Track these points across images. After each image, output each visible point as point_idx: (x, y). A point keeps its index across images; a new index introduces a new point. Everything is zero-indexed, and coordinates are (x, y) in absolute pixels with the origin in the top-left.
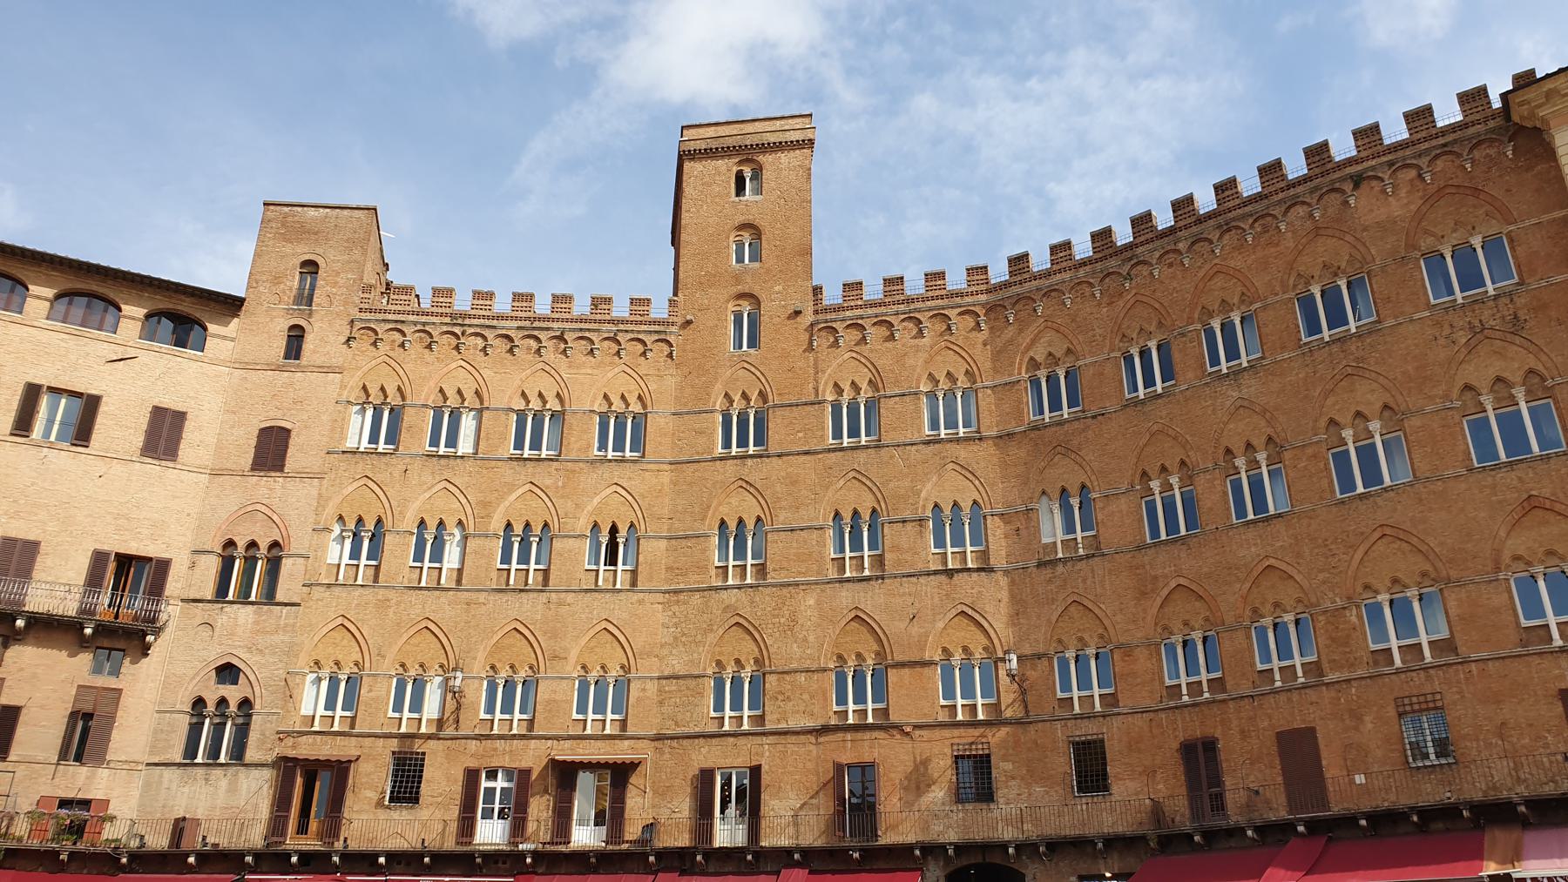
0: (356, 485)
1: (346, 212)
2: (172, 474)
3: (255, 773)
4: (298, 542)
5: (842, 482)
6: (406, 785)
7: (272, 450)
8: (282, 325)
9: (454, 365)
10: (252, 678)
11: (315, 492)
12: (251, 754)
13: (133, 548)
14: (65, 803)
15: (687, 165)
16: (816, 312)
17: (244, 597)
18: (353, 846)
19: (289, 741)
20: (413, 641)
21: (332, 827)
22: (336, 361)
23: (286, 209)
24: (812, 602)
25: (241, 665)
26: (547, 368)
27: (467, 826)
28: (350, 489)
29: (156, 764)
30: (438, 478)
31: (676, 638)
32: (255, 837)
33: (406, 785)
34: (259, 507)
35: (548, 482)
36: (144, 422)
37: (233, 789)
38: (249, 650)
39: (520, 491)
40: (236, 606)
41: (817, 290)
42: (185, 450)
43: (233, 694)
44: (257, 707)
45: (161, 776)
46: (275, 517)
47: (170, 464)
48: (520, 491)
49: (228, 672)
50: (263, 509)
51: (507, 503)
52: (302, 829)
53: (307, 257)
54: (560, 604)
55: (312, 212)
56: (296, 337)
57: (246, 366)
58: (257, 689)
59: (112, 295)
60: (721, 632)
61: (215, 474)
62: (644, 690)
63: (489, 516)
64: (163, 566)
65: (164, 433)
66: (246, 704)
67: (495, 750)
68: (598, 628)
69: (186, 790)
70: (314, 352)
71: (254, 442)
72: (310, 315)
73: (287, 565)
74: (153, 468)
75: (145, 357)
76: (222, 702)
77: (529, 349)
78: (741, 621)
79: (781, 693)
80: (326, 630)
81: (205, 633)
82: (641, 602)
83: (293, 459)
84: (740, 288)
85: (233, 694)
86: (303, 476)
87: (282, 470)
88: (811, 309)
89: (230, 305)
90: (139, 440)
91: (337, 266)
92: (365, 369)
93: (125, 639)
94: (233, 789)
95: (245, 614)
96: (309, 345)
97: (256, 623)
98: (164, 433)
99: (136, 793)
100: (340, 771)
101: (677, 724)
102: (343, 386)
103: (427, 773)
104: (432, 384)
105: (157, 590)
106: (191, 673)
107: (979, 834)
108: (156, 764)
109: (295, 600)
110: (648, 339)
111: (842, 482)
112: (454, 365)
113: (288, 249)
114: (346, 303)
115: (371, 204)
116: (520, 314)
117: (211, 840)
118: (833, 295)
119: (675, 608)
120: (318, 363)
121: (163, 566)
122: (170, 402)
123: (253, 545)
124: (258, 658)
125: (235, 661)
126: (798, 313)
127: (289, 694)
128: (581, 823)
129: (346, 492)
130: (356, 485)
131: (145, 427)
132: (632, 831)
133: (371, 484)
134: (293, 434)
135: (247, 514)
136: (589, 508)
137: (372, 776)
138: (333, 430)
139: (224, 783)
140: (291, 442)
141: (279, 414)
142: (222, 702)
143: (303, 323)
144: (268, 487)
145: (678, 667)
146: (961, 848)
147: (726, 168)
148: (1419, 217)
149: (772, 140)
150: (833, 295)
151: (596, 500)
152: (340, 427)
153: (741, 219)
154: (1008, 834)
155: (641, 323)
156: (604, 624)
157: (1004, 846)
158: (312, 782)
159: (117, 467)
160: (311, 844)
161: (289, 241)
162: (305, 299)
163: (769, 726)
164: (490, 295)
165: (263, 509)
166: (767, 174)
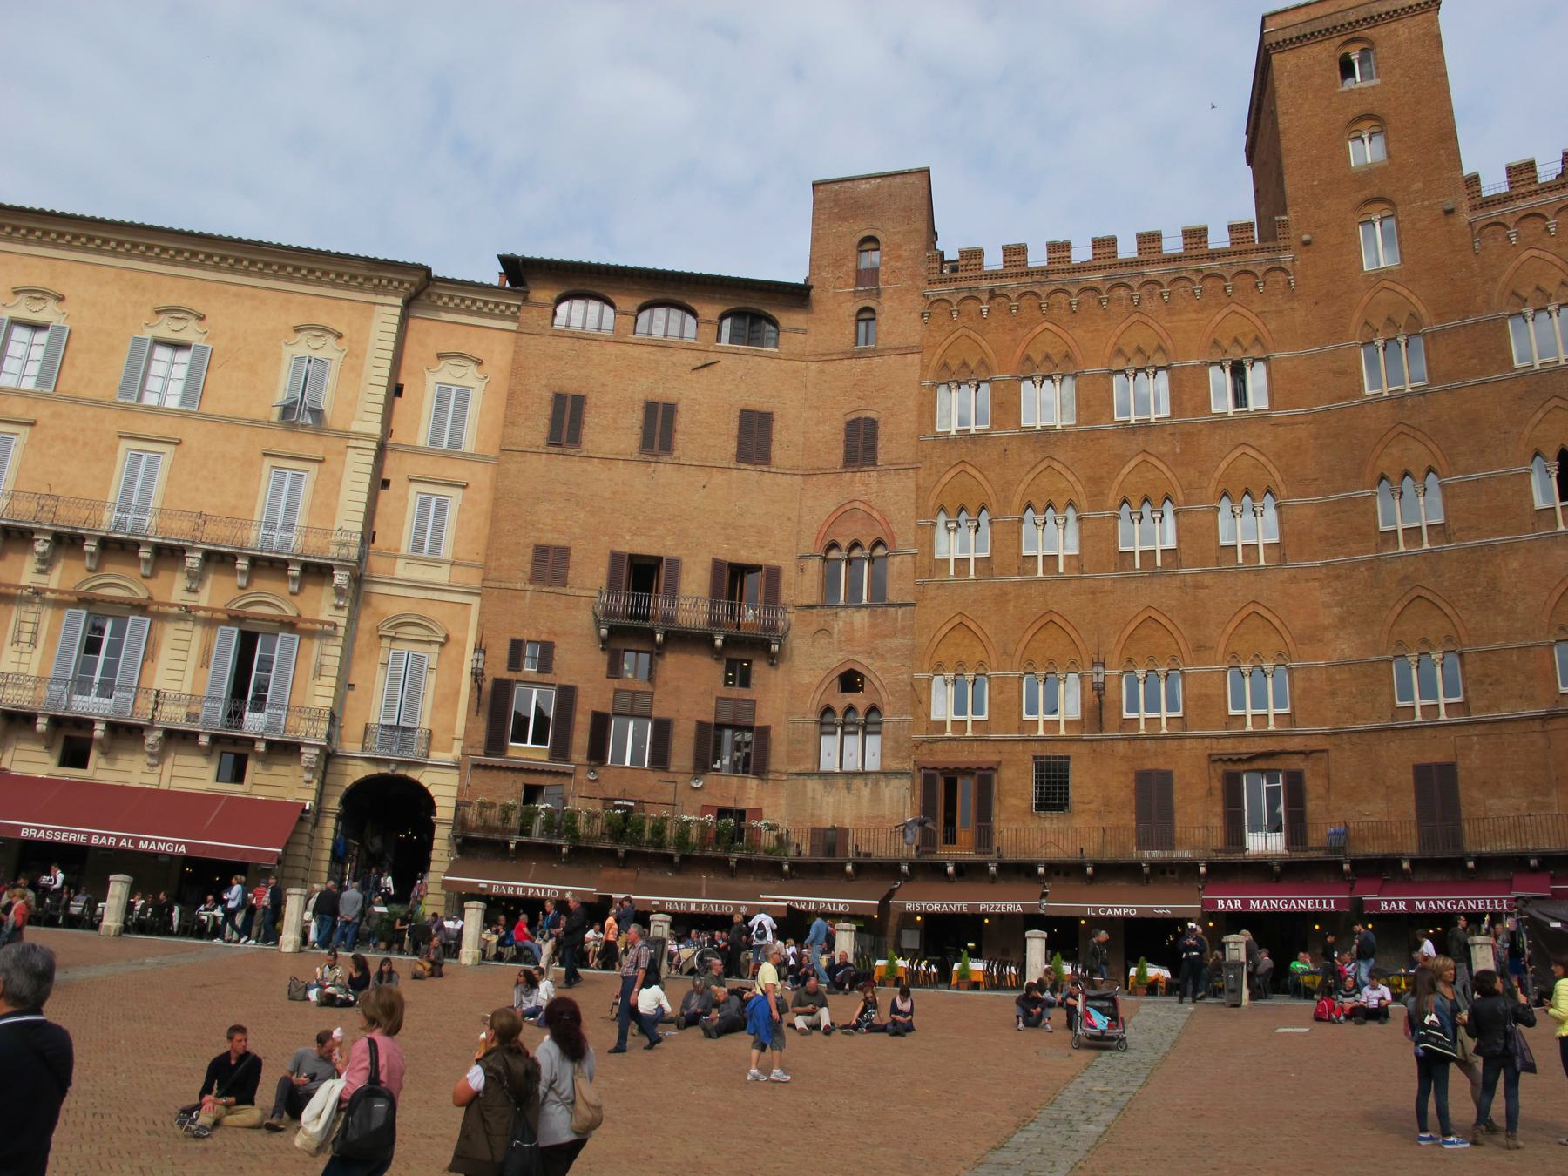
0: (953, 472)
1: (898, 180)
2: (767, 478)
3: (895, 782)
4: (905, 539)
5: (1540, 414)
6: (1053, 790)
7: (861, 442)
8: (852, 308)
9: (1038, 329)
10: (877, 684)
11: (911, 484)
13: (744, 556)
14: (722, 813)
15: (1276, 58)
16: (1474, 208)
17: (854, 602)
18: (1009, 857)
19: (925, 748)
20: (1040, 636)
21: (984, 837)
22: (915, 340)
23: (837, 187)
24: (1515, 565)
25: (864, 672)
26: (1144, 319)
28: (948, 477)
29: (799, 774)
30: (1040, 456)
31: (1342, 619)
32: (903, 849)
33: (1053, 790)
34: (857, 504)
35: (1163, 449)
36: (734, 427)
37: (876, 798)
38: (869, 654)
39: (1133, 463)
40: (850, 611)
41: (1474, 180)
42: (776, 452)
43: (859, 700)
44: (887, 713)
45: (805, 786)
46: (875, 514)
47: (765, 468)
48: (1133, 463)
49: (850, 681)
50: (861, 506)
51: (1120, 478)
52: (950, 839)
53: (866, 234)
54: (1198, 586)
55: (864, 186)
57: (823, 357)
58: (884, 695)
60: (1398, 609)
61: (809, 474)
62: (1310, 679)
63: (1102, 493)
64: (774, 574)
65: (754, 436)
66: (873, 709)
67: (1146, 751)
68: (1245, 612)
69: (831, 799)
70: (889, 334)
71: (841, 437)
72: (878, 293)
73: (894, 564)
74: (751, 474)
75: (726, 361)
76: (850, 709)
77: (1120, 299)
78: (1423, 593)
79: (1487, 675)
80: (945, 630)
81: (823, 641)
82: (1293, 579)
83: (886, 450)
84: (1366, 193)
86: (897, 468)
87: (875, 464)
88: (1465, 205)
89: (797, 296)
90: (732, 447)
91: (898, 239)
92: (945, 345)
94: (876, 798)
95: (860, 618)
96: (884, 322)
97: (873, 626)
98: (754, 436)
99: (783, 802)
100: (985, 778)
101: (1355, 717)
102: (924, 367)
103: (1074, 778)
104: (1019, 352)
105: (772, 595)
106: (816, 681)
108: (799, 774)
109: (909, 599)
110: (1259, 271)
111: (1540, 414)
112: (1038, 329)
113: (845, 228)
114: (913, 276)
115: (923, 165)
116: (1102, 262)
117: (863, 849)
118: (1494, 182)
119: (1337, 584)
120: (895, 344)
121: (774, 574)
122: (756, 403)
123: (856, 545)
124: (878, 663)
125: (858, 668)
126: (1449, 212)
127: (918, 698)
128: (1256, 828)
129: (944, 481)
130: (953, 472)
131: (735, 432)
132: (1319, 835)
133: (970, 469)
134: (880, 424)
135: (844, 513)
136: (1217, 475)
137: (1017, 787)
138: (921, 415)
139: (866, 792)
140: (880, 431)
141: (863, 405)
143: (872, 304)
144: (864, 485)
145: (1348, 652)
147: (1324, 54)
149: (1384, 10)
150: (1494, 182)
151: (1223, 465)
152: (928, 410)
153: (1356, 111)
155: (1246, 252)
156: (1251, 608)
158: (951, 790)
159: (719, 478)
160: (963, 851)
161: (845, 219)
163: (1475, 717)
164: (1067, 246)
165: (861, 506)
166: (1382, 51)
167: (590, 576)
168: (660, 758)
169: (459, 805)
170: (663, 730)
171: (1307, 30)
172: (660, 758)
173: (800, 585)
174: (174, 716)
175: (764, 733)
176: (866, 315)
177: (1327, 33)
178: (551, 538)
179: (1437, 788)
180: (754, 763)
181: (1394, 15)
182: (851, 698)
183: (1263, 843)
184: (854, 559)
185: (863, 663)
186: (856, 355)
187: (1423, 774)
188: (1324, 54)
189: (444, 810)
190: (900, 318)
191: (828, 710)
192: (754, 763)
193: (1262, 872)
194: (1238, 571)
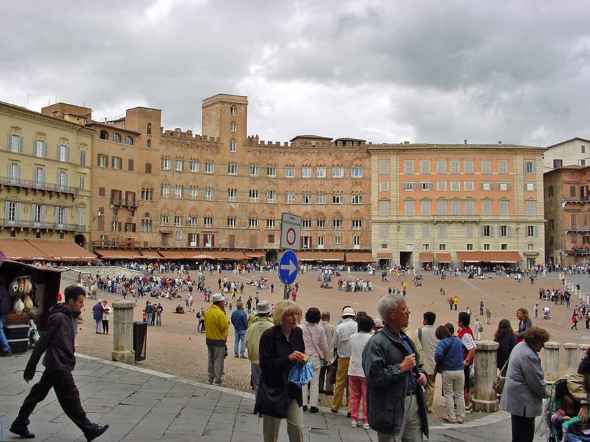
7: (149, 168)
12: (154, 230)
27: (189, 244)
43: (149, 219)
49: (147, 215)
55: (149, 111)
56: (149, 141)
57: (141, 148)
59: (120, 134)
72: (151, 137)
73: (155, 191)
85: (149, 219)
87: (150, 172)
93: (133, 209)
94: (152, 237)
96: (152, 144)
107: (271, 248)
135: (145, 182)
142: (147, 220)
144: (149, 177)
146: (270, 250)
148: (352, 161)
154: (276, 248)
157: (276, 250)
159: (126, 174)
162: (149, 132)
167: (108, 194)
168: (120, 230)
169: (90, 240)
170: (120, 224)
171: (227, 101)
172: (120, 230)
173: (138, 197)
174: (50, 226)
175: (134, 225)
176: (149, 141)
177: (231, 103)
178: (102, 186)
179: (232, 238)
180: (134, 230)
181: (241, 104)
182: (147, 218)
183: (209, 245)
184: (147, 193)
185: (149, 212)
186: (148, 149)
187: (230, 235)
188: (229, 106)
189: (87, 240)
190: (155, 142)
191: (143, 220)
192: (134, 230)
193: (208, 249)
194: (207, 201)
